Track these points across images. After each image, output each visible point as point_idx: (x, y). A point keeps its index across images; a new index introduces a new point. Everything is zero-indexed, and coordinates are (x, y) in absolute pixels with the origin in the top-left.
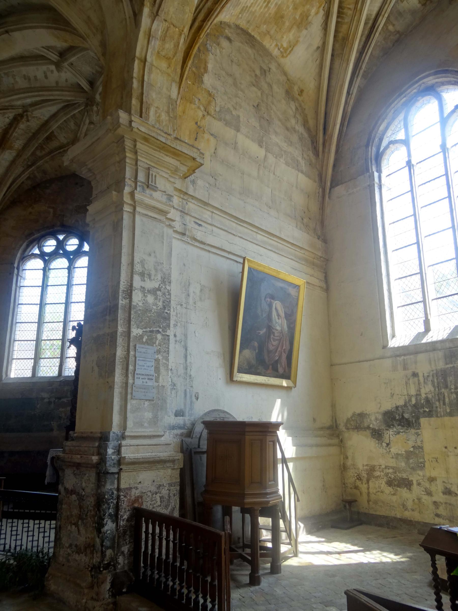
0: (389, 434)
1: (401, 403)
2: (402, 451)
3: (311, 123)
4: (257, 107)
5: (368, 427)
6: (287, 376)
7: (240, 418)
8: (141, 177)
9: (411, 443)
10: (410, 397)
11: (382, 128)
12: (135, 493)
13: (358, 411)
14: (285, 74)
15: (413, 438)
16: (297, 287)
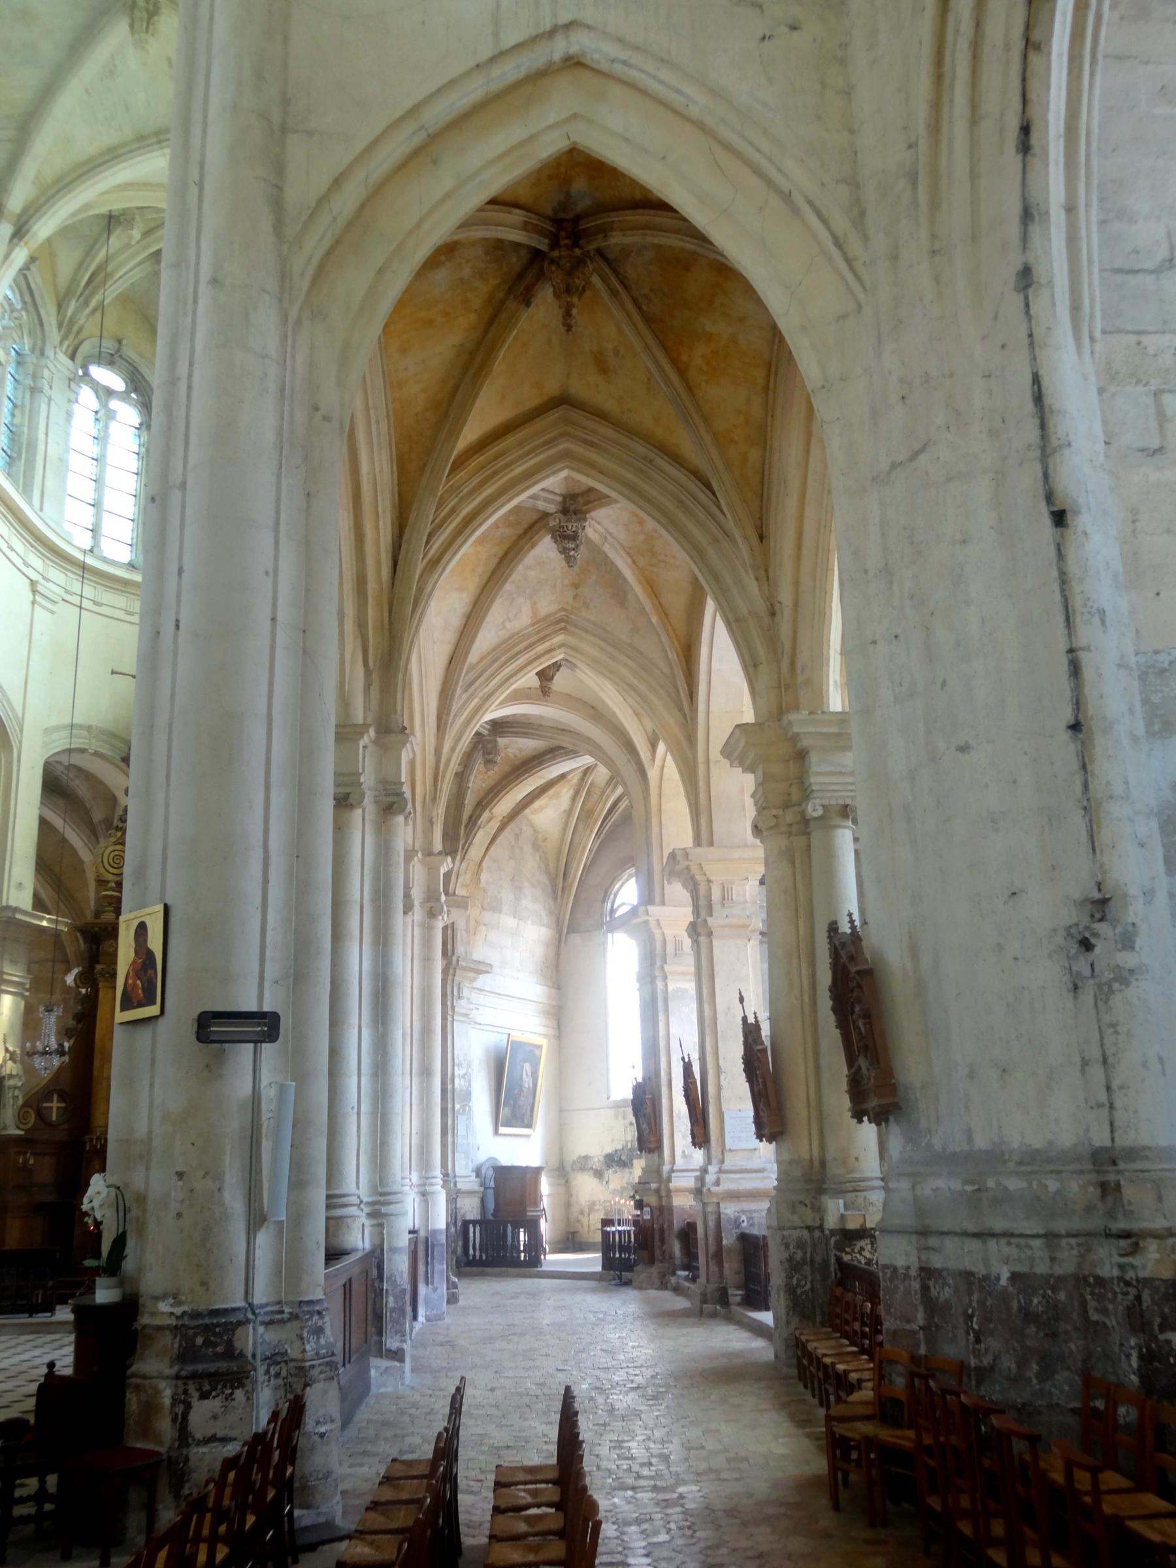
0: (609, 1174)
1: (619, 1147)
2: (618, 1187)
3: (552, 866)
4: (513, 880)
5: (592, 1168)
6: (529, 1125)
7: (504, 1164)
8: (455, 993)
9: (625, 1180)
10: (627, 1142)
11: (617, 886)
12: (463, 1211)
13: (583, 1154)
14: (532, 826)
15: (627, 1176)
16: (540, 1047)
